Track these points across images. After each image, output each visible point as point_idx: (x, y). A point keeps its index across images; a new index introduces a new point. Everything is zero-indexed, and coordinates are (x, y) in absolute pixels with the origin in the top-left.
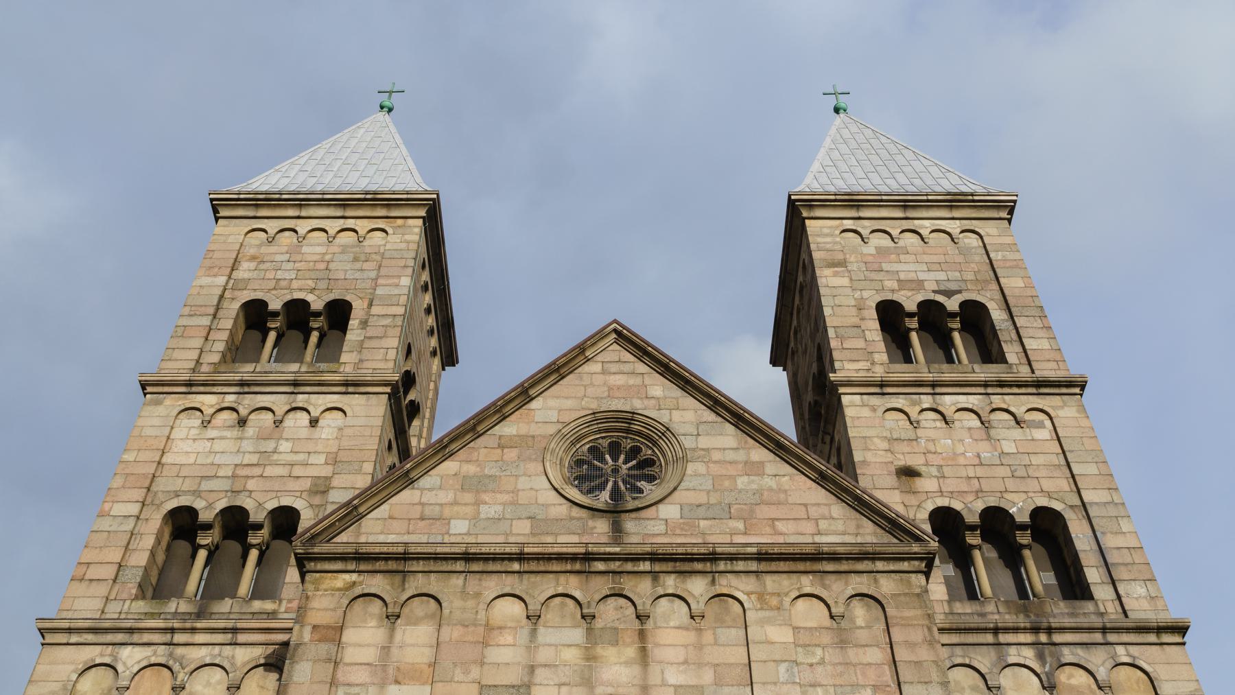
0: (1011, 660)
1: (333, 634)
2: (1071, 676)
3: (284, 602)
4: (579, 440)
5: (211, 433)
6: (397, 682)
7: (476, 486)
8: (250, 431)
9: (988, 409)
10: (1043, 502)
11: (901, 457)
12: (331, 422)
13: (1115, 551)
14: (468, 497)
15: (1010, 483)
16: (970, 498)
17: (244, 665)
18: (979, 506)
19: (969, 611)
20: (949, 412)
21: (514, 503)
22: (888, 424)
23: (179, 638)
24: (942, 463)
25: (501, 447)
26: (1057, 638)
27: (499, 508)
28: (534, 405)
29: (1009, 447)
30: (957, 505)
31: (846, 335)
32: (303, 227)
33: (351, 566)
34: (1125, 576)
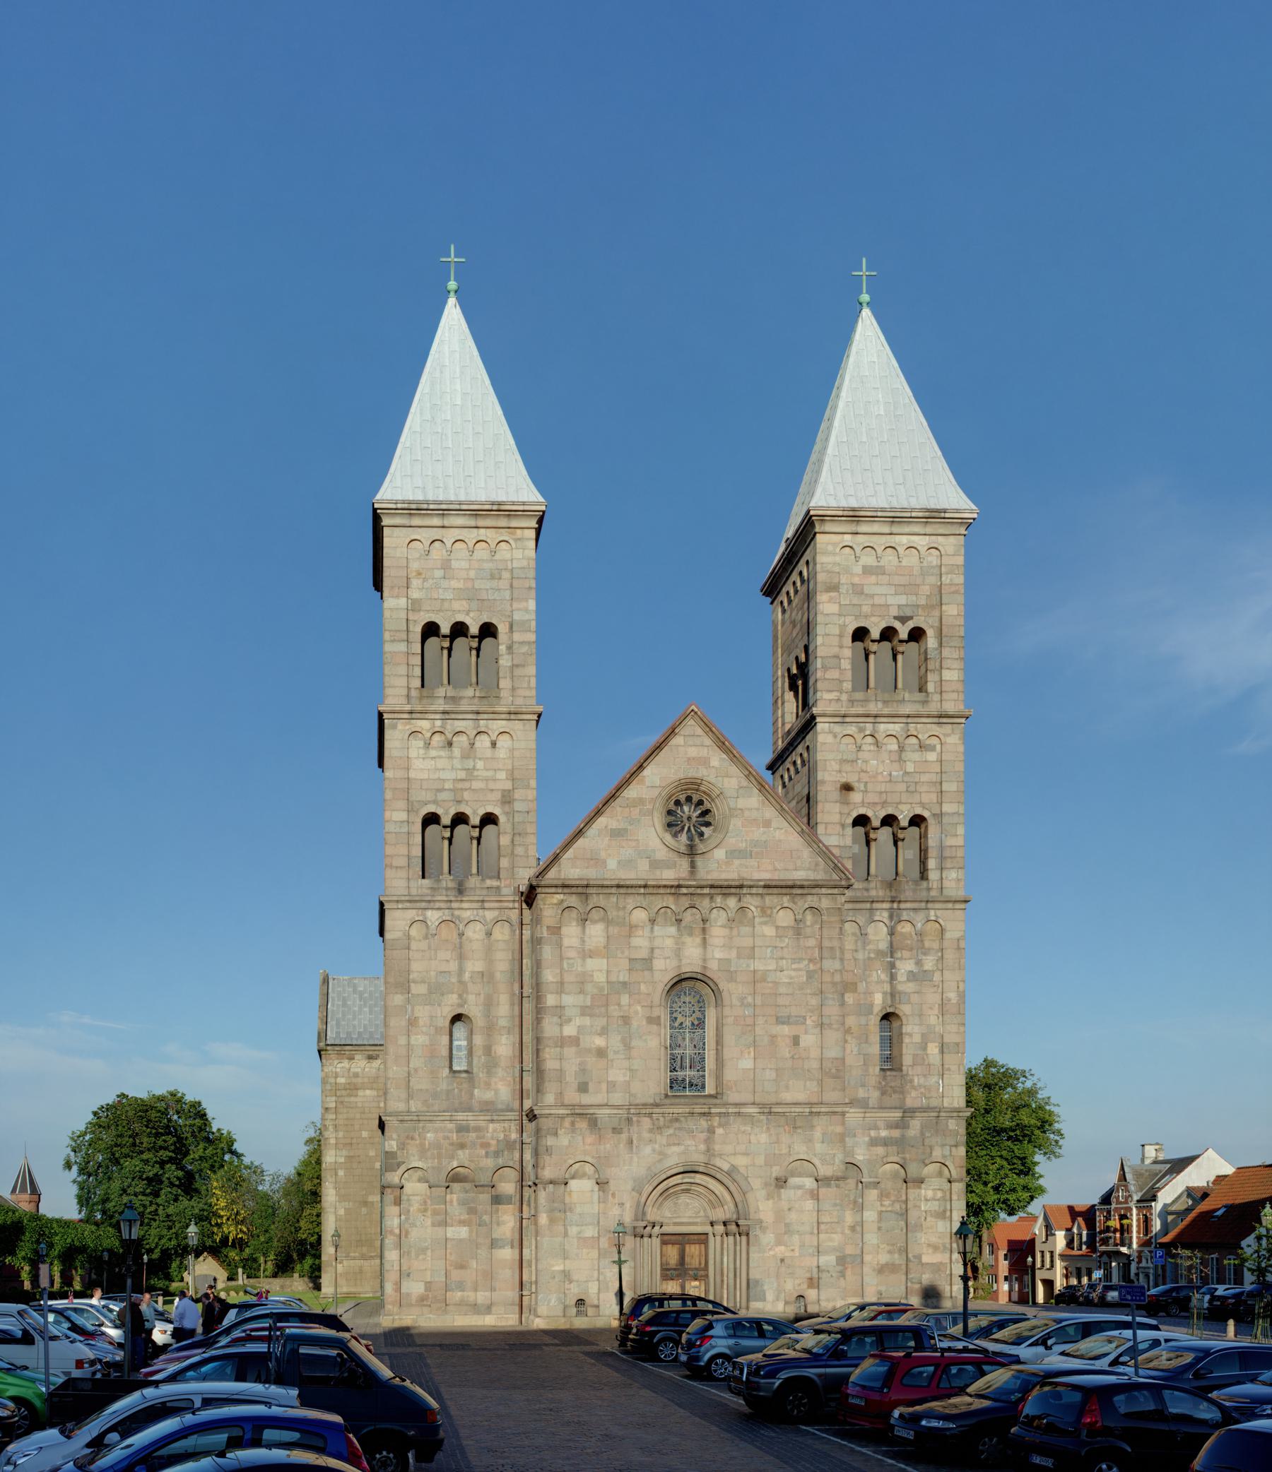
0: (876, 918)
1: (556, 930)
2: (903, 927)
3: (503, 881)
5: (433, 753)
8: (457, 752)
9: (905, 736)
10: (919, 811)
11: (844, 774)
12: (504, 742)
13: (948, 849)
15: (904, 798)
16: (879, 807)
17: (491, 921)
18: (882, 814)
19: (861, 887)
20: (880, 736)
22: (843, 747)
23: (455, 905)
24: (868, 780)
26: (903, 906)
29: (910, 767)
30: (870, 814)
31: (828, 666)
32: (449, 536)
34: (948, 865)
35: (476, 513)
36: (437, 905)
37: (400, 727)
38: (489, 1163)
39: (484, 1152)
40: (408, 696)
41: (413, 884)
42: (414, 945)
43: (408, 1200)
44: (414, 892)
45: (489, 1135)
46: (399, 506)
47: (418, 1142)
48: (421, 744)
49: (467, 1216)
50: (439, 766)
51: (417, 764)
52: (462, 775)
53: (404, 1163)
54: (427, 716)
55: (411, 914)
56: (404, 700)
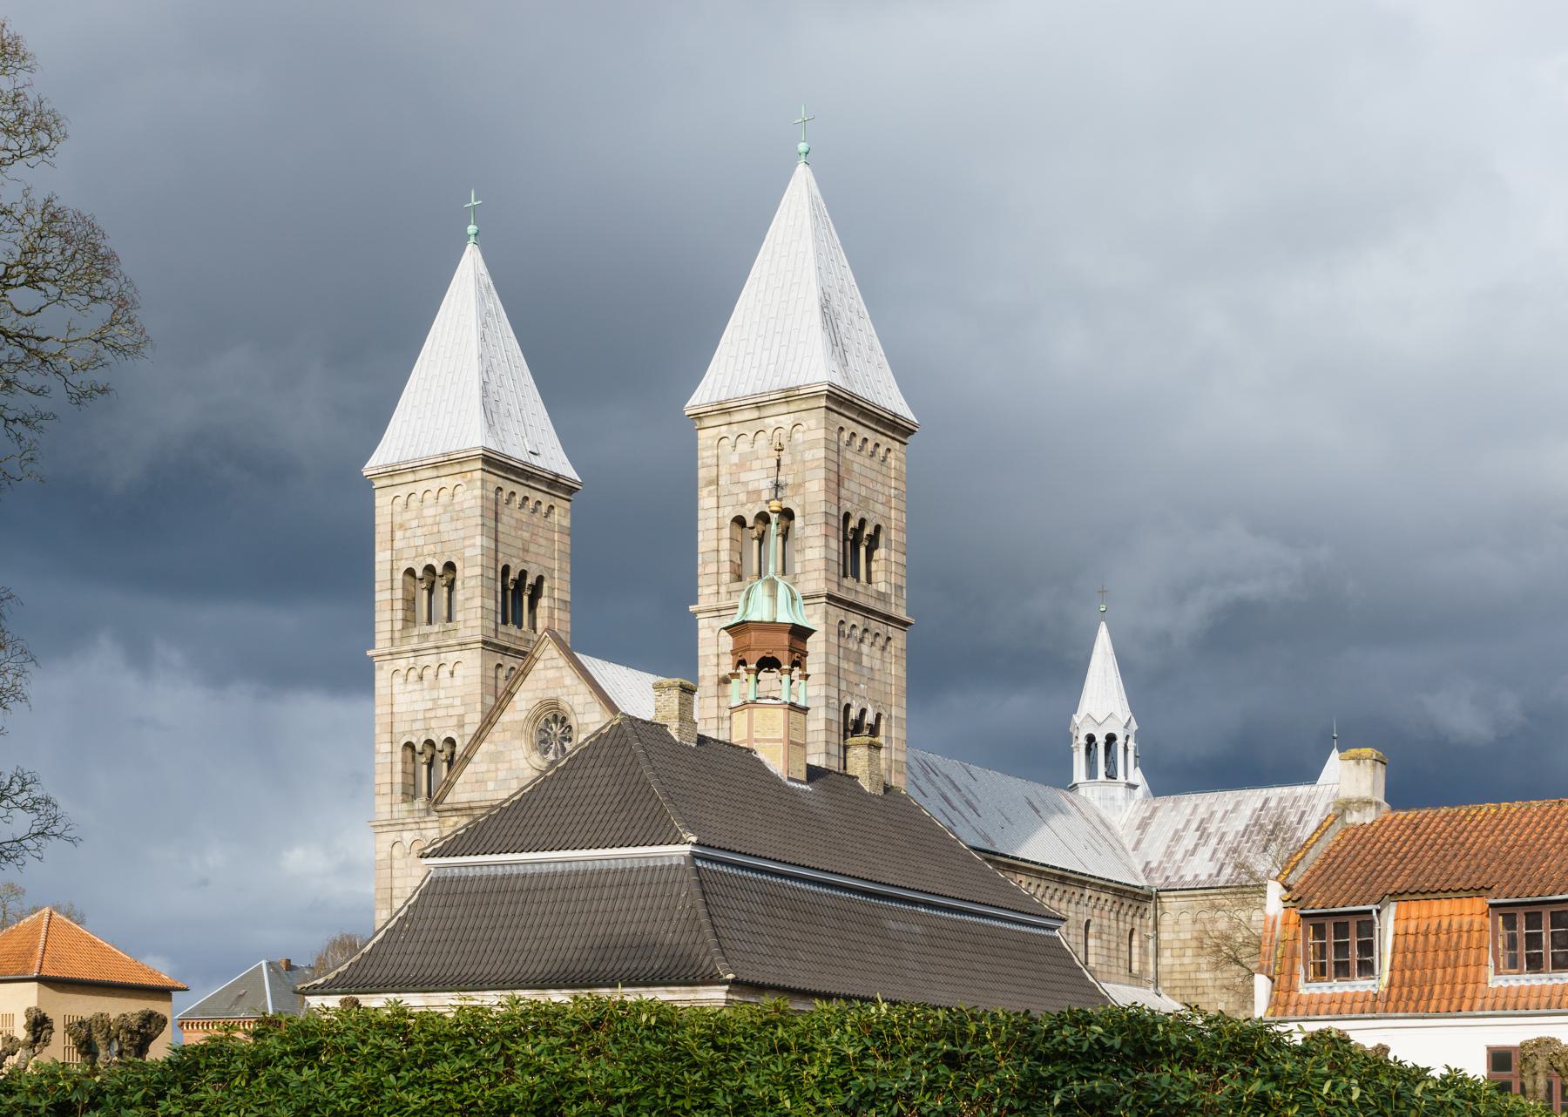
4: (537, 718)
5: (410, 687)
7: (495, 757)
8: (426, 683)
12: (459, 671)
14: (492, 767)
21: (510, 769)
23: (422, 826)
25: (504, 731)
27: (504, 773)
28: (516, 698)
33: (454, 813)
35: (435, 466)
36: (410, 826)
37: (385, 668)
40: (392, 639)
41: (395, 808)
42: (396, 864)
44: (396, 815)
46: (380, 471)
48: (401, 680)
50: (414, 699)
51: (398, 699)
52: (430, 705)
54: (404, 655)
55: (393, 836)
56: (388, 643)
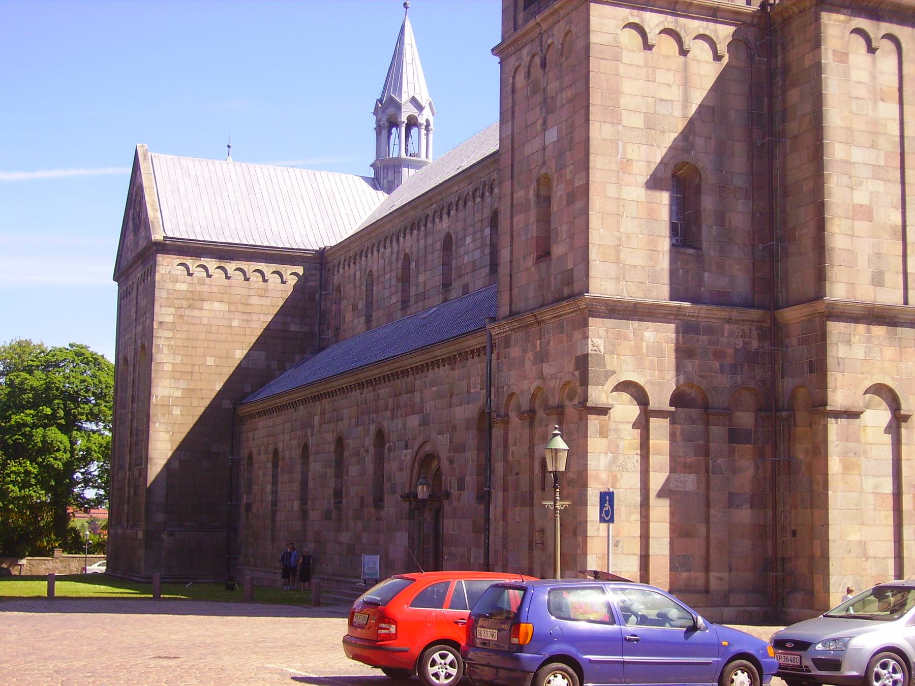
6: (882, 100)
38: (724, 381)
39: (717, 364)
43: (617, 430)
45: (724, 340)
47: (632, 343)
49: (695, 458)
53: (614, 372)
